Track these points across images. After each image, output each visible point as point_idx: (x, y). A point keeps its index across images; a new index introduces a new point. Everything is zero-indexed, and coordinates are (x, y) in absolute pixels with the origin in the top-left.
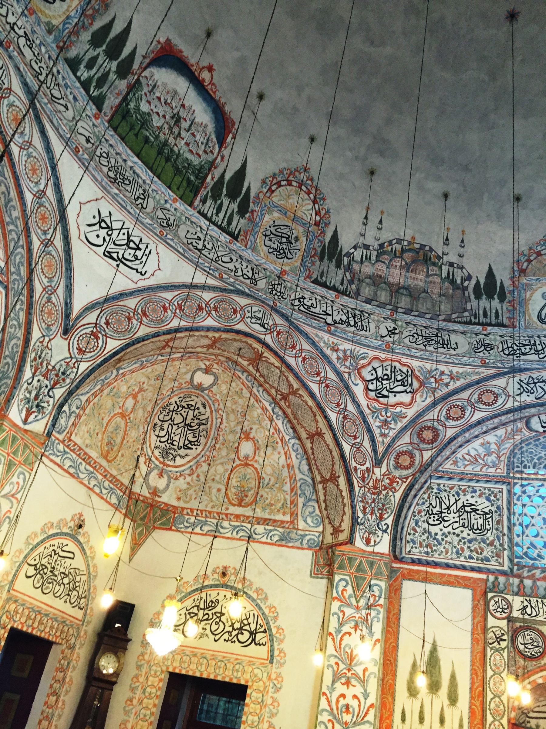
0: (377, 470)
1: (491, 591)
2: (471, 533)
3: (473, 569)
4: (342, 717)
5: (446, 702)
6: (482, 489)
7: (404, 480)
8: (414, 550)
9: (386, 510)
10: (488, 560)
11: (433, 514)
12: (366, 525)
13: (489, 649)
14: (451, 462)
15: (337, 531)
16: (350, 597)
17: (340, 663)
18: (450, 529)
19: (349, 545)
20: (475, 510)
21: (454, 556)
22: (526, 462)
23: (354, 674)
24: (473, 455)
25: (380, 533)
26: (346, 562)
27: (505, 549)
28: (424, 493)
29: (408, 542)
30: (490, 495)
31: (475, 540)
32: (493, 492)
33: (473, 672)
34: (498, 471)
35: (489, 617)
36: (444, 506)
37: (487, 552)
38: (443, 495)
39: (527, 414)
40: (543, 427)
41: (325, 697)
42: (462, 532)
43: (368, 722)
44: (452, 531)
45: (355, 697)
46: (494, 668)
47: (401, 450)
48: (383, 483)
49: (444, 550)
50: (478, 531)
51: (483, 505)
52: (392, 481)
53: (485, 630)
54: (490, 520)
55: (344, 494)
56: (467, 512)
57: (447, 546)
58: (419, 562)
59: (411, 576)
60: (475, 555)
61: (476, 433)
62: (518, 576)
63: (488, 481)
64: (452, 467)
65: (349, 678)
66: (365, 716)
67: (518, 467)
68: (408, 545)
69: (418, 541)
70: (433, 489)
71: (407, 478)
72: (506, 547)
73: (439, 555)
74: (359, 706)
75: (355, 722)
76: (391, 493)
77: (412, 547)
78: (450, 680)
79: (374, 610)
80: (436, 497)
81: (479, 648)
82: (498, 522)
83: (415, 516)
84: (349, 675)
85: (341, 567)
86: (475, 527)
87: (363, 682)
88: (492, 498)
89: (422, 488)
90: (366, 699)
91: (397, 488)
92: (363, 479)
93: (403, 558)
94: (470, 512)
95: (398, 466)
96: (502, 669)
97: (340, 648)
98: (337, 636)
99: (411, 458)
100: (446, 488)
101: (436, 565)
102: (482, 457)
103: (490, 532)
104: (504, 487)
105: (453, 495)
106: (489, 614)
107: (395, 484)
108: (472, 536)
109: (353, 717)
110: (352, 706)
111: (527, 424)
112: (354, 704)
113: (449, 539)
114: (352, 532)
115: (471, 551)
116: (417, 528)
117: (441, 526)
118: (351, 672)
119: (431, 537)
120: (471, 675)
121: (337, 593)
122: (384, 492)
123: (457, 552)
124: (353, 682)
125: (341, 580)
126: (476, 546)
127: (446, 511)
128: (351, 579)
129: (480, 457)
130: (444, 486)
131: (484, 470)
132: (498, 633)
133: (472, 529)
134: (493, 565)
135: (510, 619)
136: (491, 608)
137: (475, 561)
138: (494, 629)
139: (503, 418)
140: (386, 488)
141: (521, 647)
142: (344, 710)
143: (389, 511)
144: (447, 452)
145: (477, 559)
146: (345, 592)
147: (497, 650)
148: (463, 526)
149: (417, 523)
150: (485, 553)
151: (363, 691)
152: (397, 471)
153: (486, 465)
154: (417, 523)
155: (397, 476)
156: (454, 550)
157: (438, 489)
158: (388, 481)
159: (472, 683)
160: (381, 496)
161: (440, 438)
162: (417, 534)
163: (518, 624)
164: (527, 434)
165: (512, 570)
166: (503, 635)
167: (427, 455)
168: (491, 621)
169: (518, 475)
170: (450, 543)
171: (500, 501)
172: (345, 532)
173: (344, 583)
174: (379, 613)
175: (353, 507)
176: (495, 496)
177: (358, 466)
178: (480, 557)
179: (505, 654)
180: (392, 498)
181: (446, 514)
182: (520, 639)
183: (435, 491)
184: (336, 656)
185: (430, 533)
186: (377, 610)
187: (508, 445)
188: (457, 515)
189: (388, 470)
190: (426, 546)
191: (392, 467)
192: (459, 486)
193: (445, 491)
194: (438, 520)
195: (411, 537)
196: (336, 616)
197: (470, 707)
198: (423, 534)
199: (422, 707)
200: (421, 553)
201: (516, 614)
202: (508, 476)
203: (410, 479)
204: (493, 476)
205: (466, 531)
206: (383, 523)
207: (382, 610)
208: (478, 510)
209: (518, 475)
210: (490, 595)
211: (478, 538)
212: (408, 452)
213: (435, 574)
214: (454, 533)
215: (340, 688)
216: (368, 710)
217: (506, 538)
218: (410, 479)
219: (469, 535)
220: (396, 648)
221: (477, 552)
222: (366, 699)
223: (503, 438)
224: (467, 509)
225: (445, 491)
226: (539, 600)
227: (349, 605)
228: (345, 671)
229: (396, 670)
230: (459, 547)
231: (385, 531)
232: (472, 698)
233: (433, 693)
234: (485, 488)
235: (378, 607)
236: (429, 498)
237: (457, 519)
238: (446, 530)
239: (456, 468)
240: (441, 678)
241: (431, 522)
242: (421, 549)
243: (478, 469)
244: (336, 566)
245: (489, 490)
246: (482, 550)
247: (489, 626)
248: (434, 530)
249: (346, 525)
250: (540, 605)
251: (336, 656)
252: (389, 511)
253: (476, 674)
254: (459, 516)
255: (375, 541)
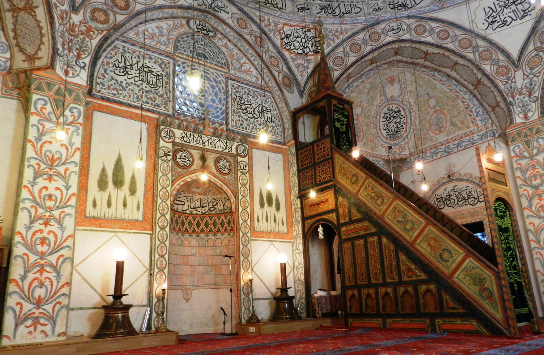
0: (73, 16)
1: (163, 125)
2: (147, 86)
3: (148, 110)
4: (45, 203)
5: (128, 193)
6: (157, 59)
7: (100, 32)
8: (103, 90)
9: (83, 51)
10: (159, 106)
11: (119, 67)
12: (65, 59)
13: (160, 160)
14: (134, 33)
15: (31, 58)
16: (49, 113)
17: (41, 163)
18: (132, 80)
19: (50, 71)
20: (152, 72)
21: (135, 100)
22: (186, 48)
23: (56, 172)
24: (150, 32)
25: (78, 68)
26: (44, 86)
27: (170, 101)
28: (112, 50)
29: (98, 84)
30: (162, 64)
31: (151, 91)
32: (164, 62)
33: (147, 175)
34: (168, 49)
35: (161, 141)
36: (128, 64)
37: (159, 101)
38: (128, 55)
39: (189, 15)
40: (197, 28)
41: (26, 189)
42: (141, 84)
43: (70, 206)
44: (134, 82)
45: (57, 188)
46: (163, 171)
47: (97, 6)
48: (80, 29)
49: (127, 95)
50: (153, 86)
51: (157, 69)
52: (89, 29)
53: (156, 148)
54: (161, 80)
55: (43, 24)
56: (145, 72)
57: (130, 92)
58: (108, 100)
59: (101, 109)
60: (150, 101)
61: (155, 16)
62: (178, 119)
63: (161, 54)
64: (135, 36)
65: (51, 175)
66: (67, 202)
67: (180, 50)
68: (98, 86)
69: (107, 84)
70: (119, 48)
71: (102, 31)
72: (171, 99)
73: (124, 97)
74: (62, 195)
75: (58, 207)
76: (87, 39)
77: (102, 88)
78: (131, 180)
79: (74, 126)
80: (122, 56)
81: (152, 161)
82: (167, 83)
83: (104, 65)
84: (51, 172)
85: (38, 88)
86: (151, 83)
87: (64, 178)
88: (163, 66)
89: (110, 45)
90: (67, 190)
91: (94, 36)
92: (62, 18)
93: (94, 94)
94: (148, 72)
95: (93, 19)
96: (168, 172)
97: (41, 153)
98: (37, 143)
99: (106, 16)
100: (130, 51)
101: (121, 103)
102: (157, 36)
103: (161, 88)
104: (171, 61)
105: (135, 57)
106: (161, 139)
107: (91, 33)
108: (149, 88)
109: (56, 202)
110: (54, 195)
111: (188, 22)
112: (58, 194)
113: (131, 87)
114: (53, 59)
115: (148, 98)
116: (105, 75)
117: (125, 77)
118: (52, 171)
119: (118, 83)
120: (146, 177)
121: (36, 109)
122: (81, 37)
123: (138, 98)
124: (55, 178)
125: (39, 99)
126: (151, 96)
127: (129, 67)
128: (50, 99)
129: (155, 35)
130: (128, 49)
131: (158, 45)
132: (166, 151)
133: (148, 84)
134: (162, 109)
135: (174, 144)
136: (163, 135)
137: (150, 105)
138: (164, 149)
139: (175, 11)
140: (82, 34)
141: (179, 161)
142: (47, 198)
143: (87, 53)
144: (133, 23)
145: (152, 104)
146: (44, 110)
147: (165, 161)
148: (142, 80)
149: (105, 71)
150: (157, 101)
151: (64, 184)
152: (93, 23)
153: (159, 42)
154: (105, 71)
155: (93, 26)
156: (135, 96)
157: (124, 50)
158: (84, 28)
159: (146, 181)
160: (79, 39)
161: (131, 8)
162: (105, 80)
163: (177, 148)
164: (187, 29)
165: (174, 115)
166: (169, 152)
167: (120, 18)
168: (162, 143)
169: (180, 55)
170: (132, 90)
171: (169, 69)
172: (44, 59)
173: (43, 103)
174: (78, 129)
175: (54, 38)
176: (165, 65)
177: (58, 5)
178: (154, 103)
179: (170, 164)
180: (89, 43)
181: (129, 70)
182: (178, 156)
183: (121, 50)
184: (36, 159)
185: (116, 81)
186: (76, 127)
187: (175, 33)
188: (138, 72)
189: (84, 19)
190: (113, 89)
191: (88, 18)
192: (140, 52)
193: (129, 53)
194: (123, 72)
195: (101, 80)
196: (35, 128)
197: (144, 196)
198: (111, 80)
199: (109, 197)
200: (109, 93)
201: (178, 140)
202: (174, 55)
203: (105, 32)
204: (165, 51)
205: (145, 84)
206: (81, 61)
207: (81, 127)
208: (153, 72)
209: (180, 55)
210: (162, 127)
211: (153, 90)
212: (103, 10)
213: (121, 110)
214: (135, 84)
215: (42, 182)
216: (70, 197)
217: (171, 94)
218: (105, 32)
219: (146, 87)
220: (88, 158)
221: (152, 100)
222: (67, 190)
223: (171, 27)
224: (145, 69)
225: (129, 53)
226: (192, 133)
227: (49, 120)
228: (46, 170)
229: (88, 173)
230: (139, 94)
231: (83, 68)
232: (146, 190)
233: (118, 188)
234: (158, 58)
235: (77, 125)
236: (116, 54)
237: (138, 75)
238: (129, 81)
239: (137, 38)
240: (124, 179)
241: (117, 72)
242: (110, 91)
243: (154, 43)
244: (33, 87)
245: (161, 60)
246: (155, 99)
247: (161, 146)
248: (120, 79)
249: (45, 53)
250: (192, 137)
251: (36, 159)
252: (87, 53)
253: (149, 176)
254: (139, 73)
255: (73, 74)
